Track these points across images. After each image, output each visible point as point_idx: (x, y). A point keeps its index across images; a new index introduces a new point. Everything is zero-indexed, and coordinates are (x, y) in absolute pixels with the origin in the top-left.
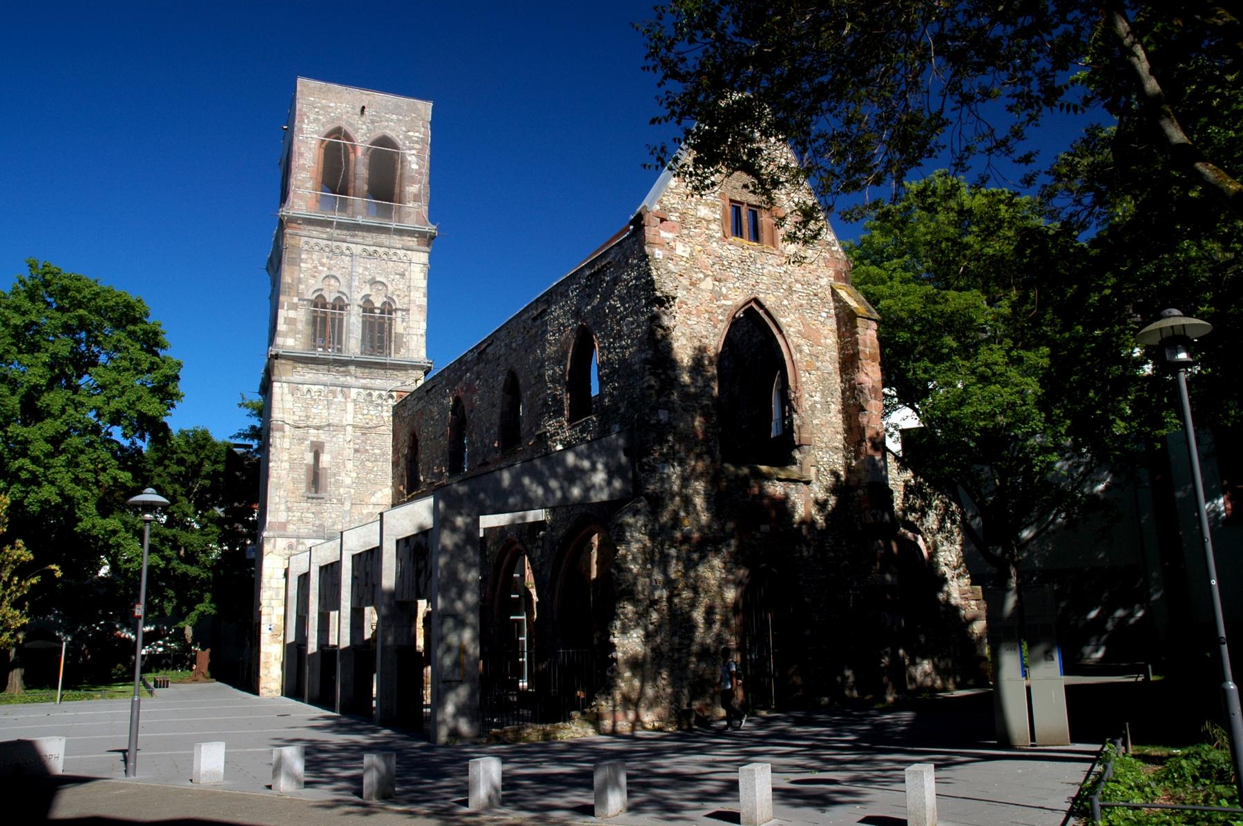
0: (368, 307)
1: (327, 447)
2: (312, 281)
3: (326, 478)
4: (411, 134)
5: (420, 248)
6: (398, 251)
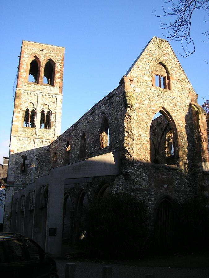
0: (43, 112)
1: (28, 157)
2: (25, 104)
3: (27, 168)
5: (60, 94)
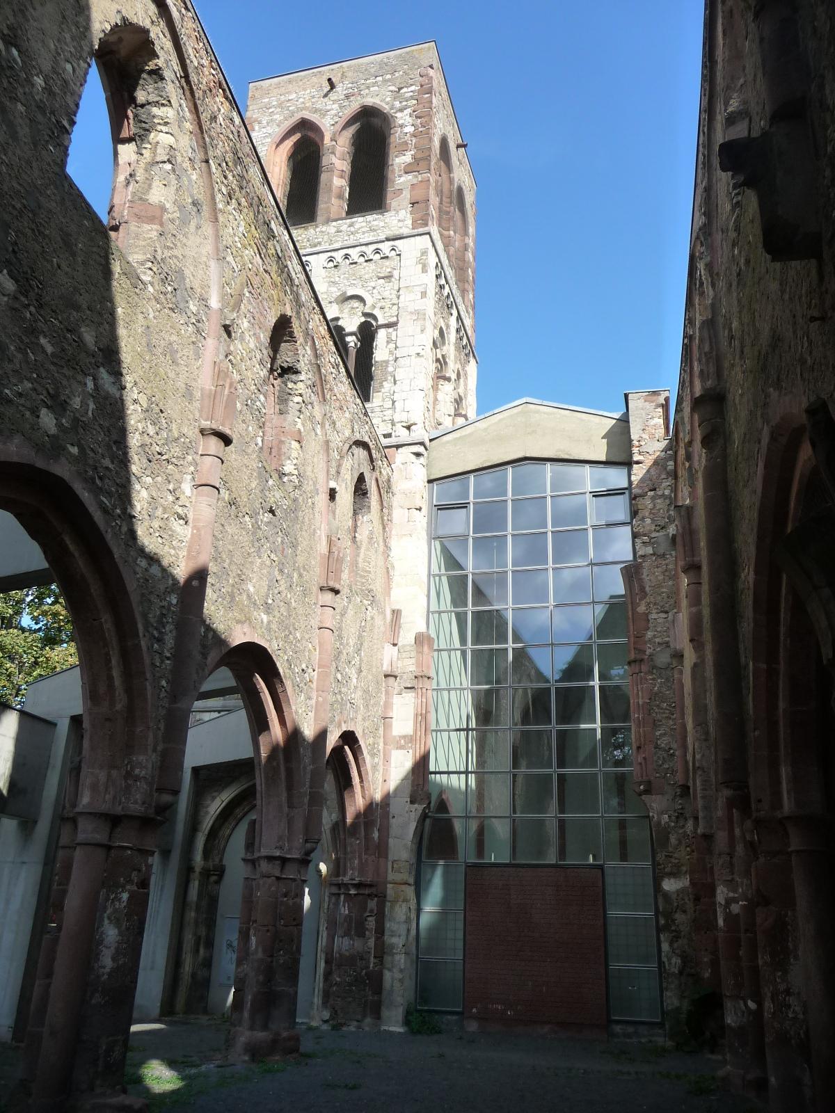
4: (402, 91)
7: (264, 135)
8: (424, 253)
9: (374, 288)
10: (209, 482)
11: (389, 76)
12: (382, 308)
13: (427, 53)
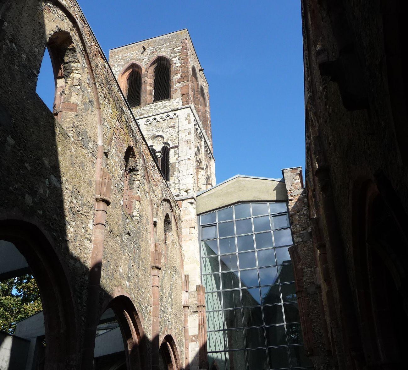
4: (174, 50)
6: (169, 114)
7: (116, 71)
8: (188, 115)
9: (167, 132)
10: (100, 223)
11: (168, 44)
12: (171, 140)
13: (184, 34)
